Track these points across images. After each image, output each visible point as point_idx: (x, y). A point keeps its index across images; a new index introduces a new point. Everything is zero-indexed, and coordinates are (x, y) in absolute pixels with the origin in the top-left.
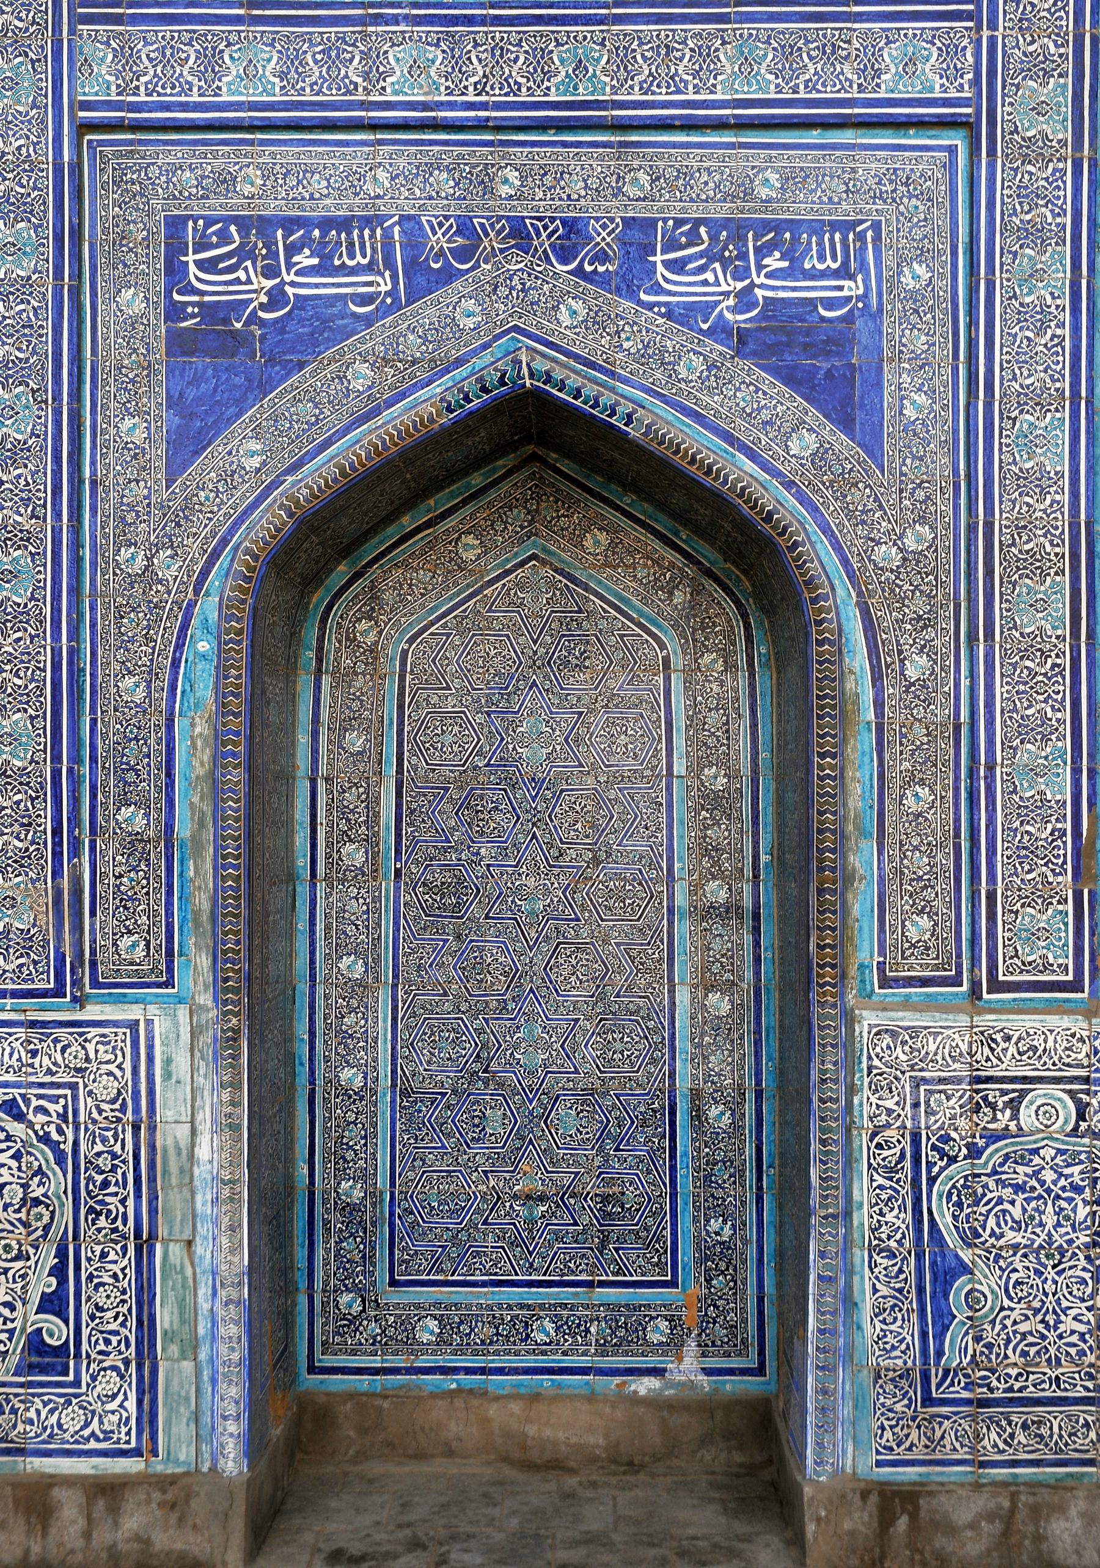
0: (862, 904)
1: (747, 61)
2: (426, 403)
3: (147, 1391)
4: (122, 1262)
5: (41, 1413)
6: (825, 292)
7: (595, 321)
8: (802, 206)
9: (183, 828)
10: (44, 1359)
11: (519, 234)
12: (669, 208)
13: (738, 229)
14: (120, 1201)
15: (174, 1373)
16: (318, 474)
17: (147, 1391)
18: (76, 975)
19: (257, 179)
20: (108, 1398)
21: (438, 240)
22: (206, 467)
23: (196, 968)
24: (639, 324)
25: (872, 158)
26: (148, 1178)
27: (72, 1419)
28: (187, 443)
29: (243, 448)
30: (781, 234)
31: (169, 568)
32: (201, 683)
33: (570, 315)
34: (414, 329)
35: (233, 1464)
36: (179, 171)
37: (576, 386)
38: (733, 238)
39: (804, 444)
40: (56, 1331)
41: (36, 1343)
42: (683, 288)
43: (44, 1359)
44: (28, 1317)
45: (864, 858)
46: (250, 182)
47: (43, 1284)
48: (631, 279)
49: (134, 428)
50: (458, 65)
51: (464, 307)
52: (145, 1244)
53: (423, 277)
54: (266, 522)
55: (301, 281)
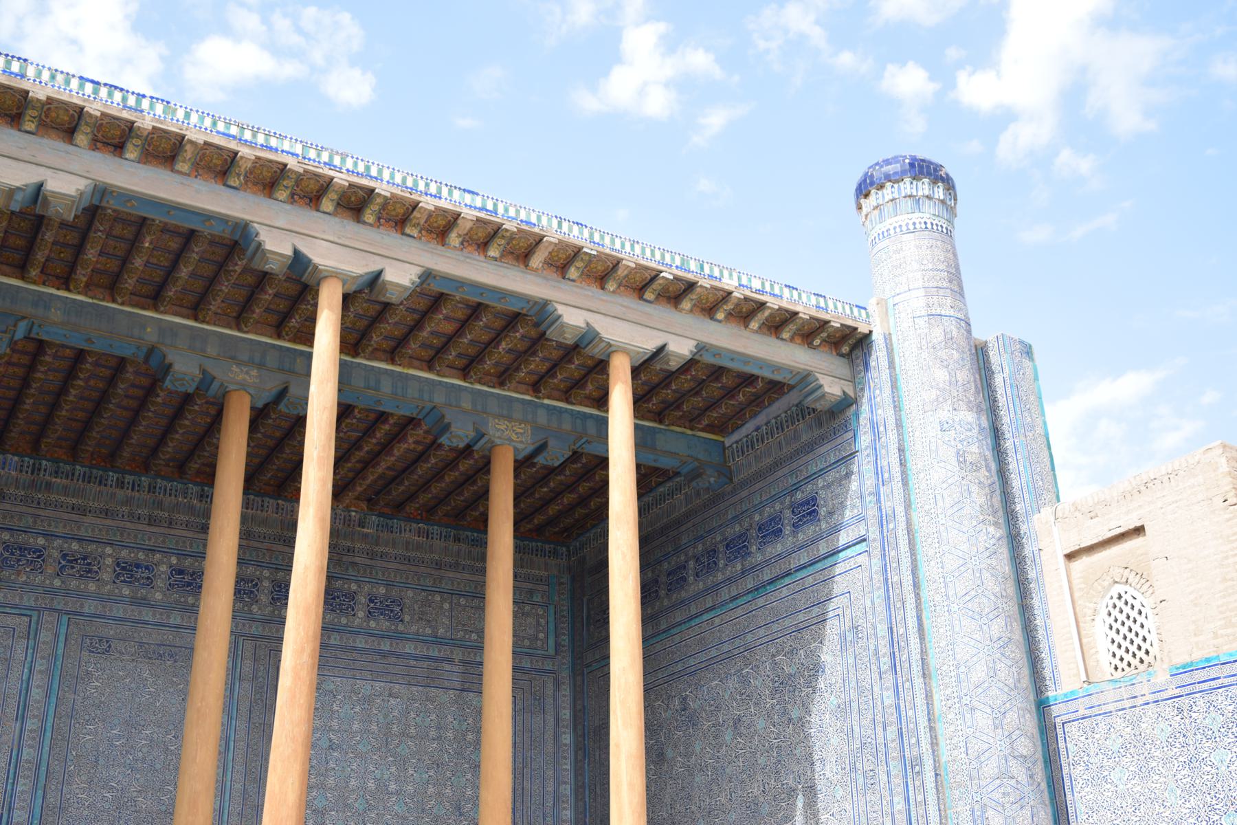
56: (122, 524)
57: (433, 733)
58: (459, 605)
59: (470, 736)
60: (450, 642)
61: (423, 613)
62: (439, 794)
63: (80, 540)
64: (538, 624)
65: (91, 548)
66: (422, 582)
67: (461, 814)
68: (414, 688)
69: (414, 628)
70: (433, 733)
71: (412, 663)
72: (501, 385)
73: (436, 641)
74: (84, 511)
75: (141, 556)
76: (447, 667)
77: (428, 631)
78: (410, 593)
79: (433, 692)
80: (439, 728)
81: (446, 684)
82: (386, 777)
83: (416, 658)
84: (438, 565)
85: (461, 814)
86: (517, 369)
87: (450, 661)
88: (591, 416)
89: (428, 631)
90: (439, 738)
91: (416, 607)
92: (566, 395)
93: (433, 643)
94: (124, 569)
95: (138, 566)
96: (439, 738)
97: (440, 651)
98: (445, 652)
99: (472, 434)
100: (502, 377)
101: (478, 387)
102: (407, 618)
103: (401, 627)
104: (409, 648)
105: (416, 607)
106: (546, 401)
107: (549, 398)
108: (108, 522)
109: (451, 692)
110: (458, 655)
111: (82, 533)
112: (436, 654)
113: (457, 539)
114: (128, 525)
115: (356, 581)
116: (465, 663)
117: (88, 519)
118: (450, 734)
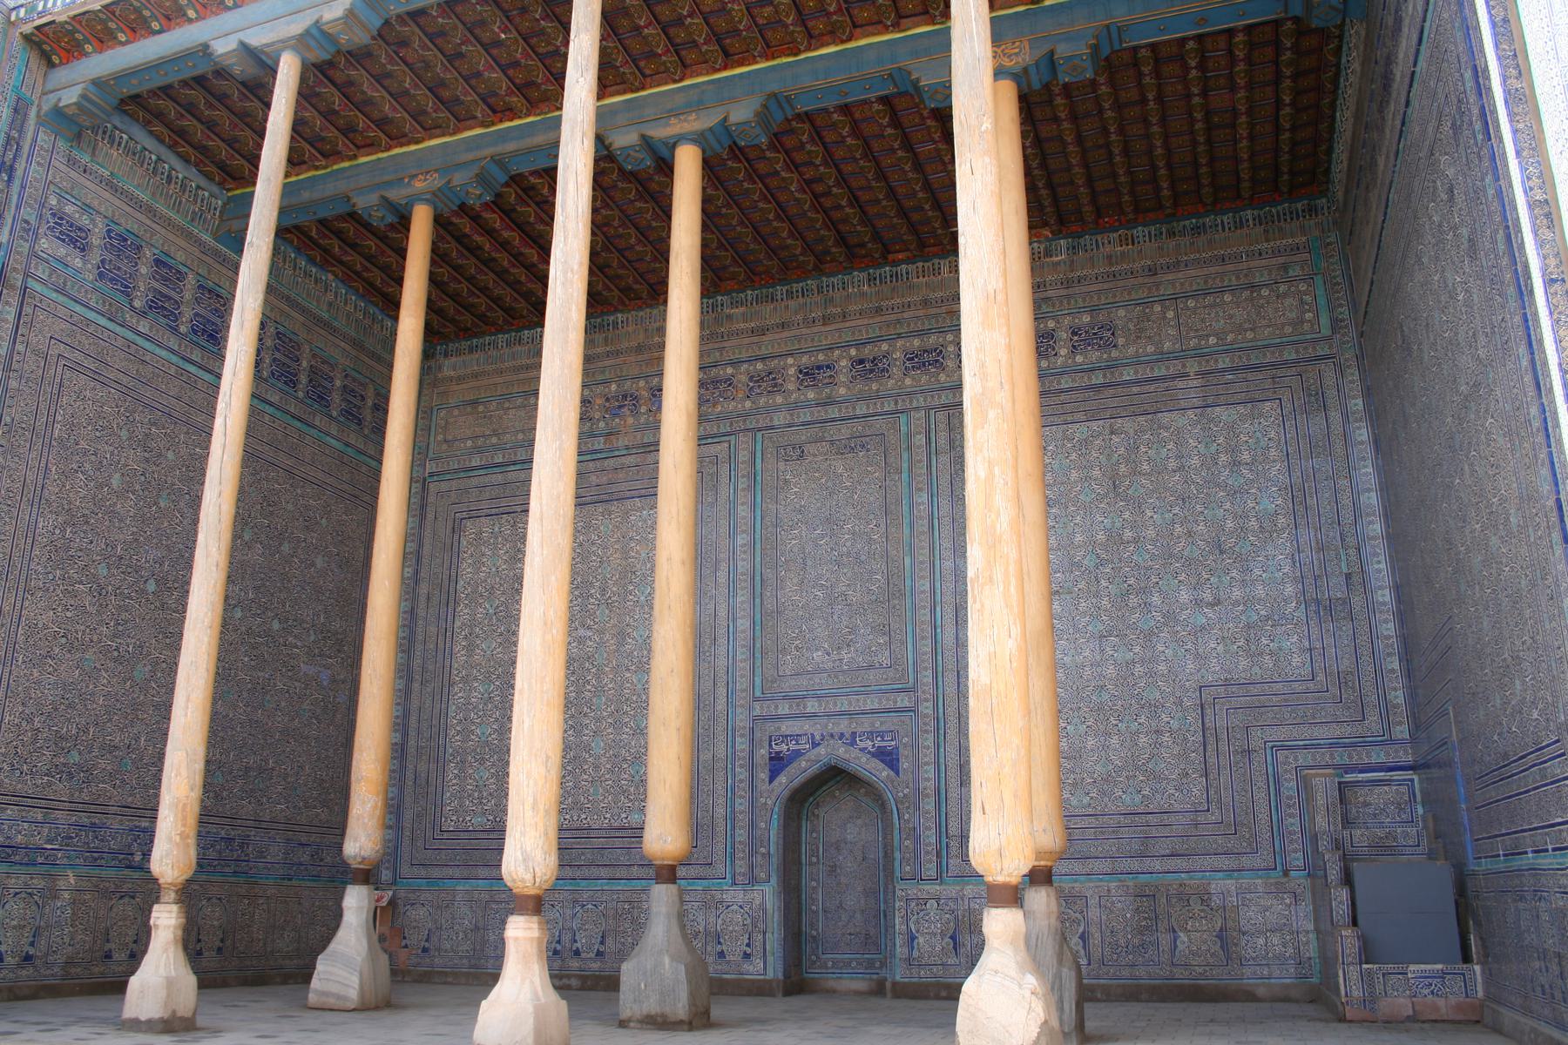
0: (897, 864)
2: (814, 770)
4: (760, 937)
5: (746, 967)
10: (747, 956)
11: (832, 736)
14: (761, 926)
15: (770, 959)
16: (796, 783)
18: (753, 880)
19: (786, 728)
21: (818, 738)
22: (776, 783)
23: (774, 880)
28: (771, 780)
29: (782, 779)
32: (775, 823)
34: (813, 754)
35: (781, 976)
36: (770, 727)
40: (749, 950)
45: (897, 855)
46: (784, 728)
49: (763, 775)
51: (822, 750)
53: (815, 745)
54: (786, 793)
55: (793, 746)
56: (797, 332)
57: (1172, 464)
58: (1188, 308)
60: (1182, 355)
61: (1141, 330)
62: (1190, 534)
64: (1302, 302)
65: (774, 363)
66: (1134, 296)
67: (1222, 552)
68: (1141, 418)
69: (1131, 350)
71: (1135, 390)
73: (1162, 357)
74: (763, 331)
75: (821, 357)
76: (1181, 385)
77: (1150, 349)
78: (1122, 313)
79: (1165, 418)
80: (1179, 457)
81: (1183, 404)
82: (1118, 525)
83: (1138, 382)
84: (1152, 271)
85: (1222, 552)
87: (1185, 375)
89: (1150, 349)
90: (1181, 468)
93: (1158, 361)
94: (806, 374)
95: (819, 368)
96: (1181, 468)
97: (1168, 368)
98: (1175, 367)
102: (1121, 341)
103: (1115, 353)
104: (1128, 375)
108: (786, 334)
109: (1190, 412)
110: (1193, 367)
111: (764, 351)
112: (1163, 372)
114: (804, 331)
115: (1053, 318)
116: (1202, 374)
118: (1195, 461)
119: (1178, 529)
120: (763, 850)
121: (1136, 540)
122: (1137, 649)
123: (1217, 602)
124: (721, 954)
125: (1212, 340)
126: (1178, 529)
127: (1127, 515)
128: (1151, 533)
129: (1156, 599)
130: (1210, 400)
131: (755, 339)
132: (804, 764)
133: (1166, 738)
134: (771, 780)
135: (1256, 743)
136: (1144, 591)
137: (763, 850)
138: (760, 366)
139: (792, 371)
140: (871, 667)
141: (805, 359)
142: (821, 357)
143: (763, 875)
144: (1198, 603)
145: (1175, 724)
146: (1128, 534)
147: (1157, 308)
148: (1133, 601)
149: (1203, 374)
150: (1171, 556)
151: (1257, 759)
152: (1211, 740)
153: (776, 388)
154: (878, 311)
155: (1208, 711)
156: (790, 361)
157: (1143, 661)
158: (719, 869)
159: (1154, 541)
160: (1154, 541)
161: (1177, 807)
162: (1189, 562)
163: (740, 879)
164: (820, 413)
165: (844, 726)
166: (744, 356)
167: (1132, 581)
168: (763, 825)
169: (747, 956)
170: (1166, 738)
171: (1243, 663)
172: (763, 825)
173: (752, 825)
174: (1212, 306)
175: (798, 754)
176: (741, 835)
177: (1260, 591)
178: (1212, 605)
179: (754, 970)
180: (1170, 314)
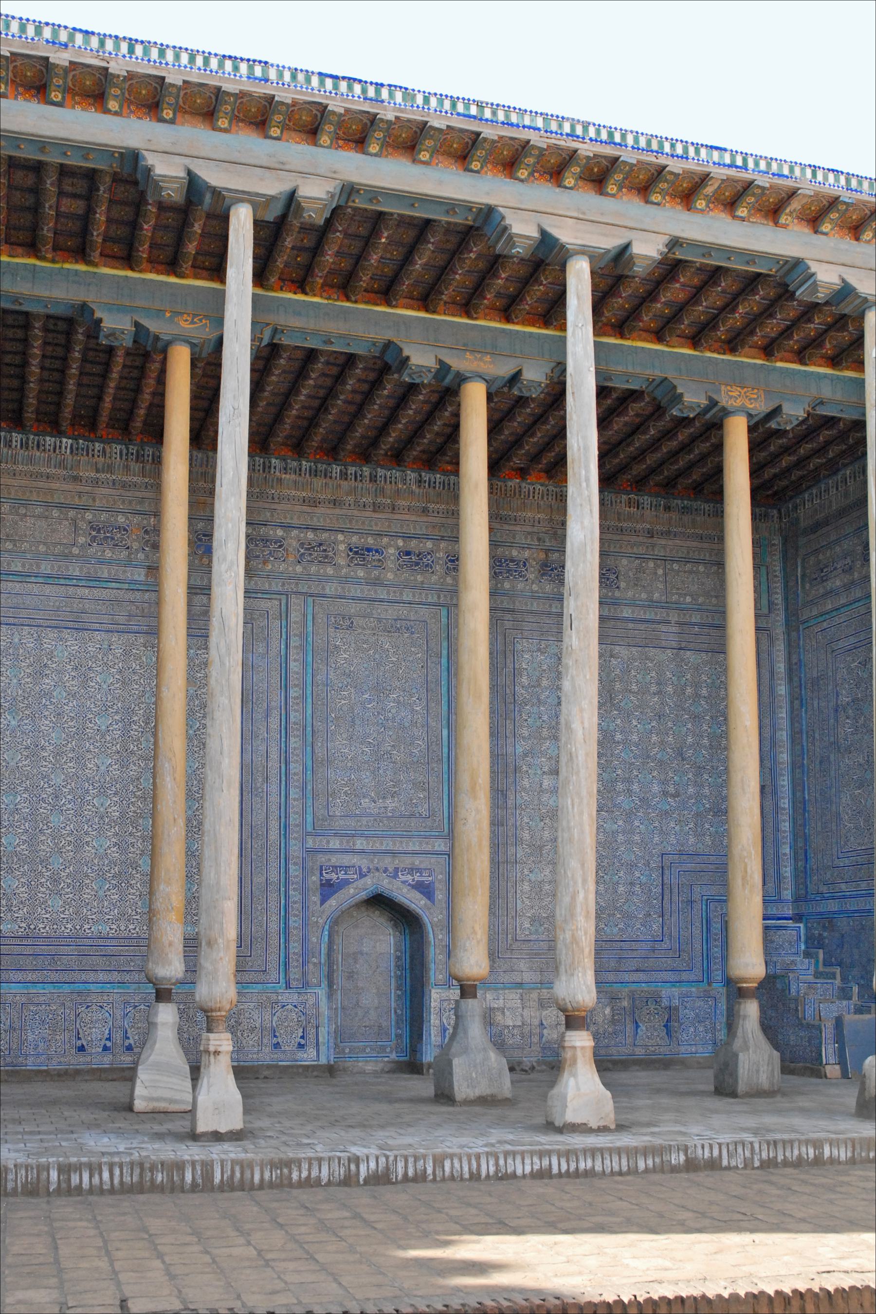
1: (414, 844)
3: (318, 1051)
5: (300, 1055)
6: (426, 879)
7: (389, 883)
8: (422, 866)
9: (323, 961)
11: (377, 869)
12: (402, 866)
13: (412, 869)
17: (318, 1051)
20: (312, 1053)
21: (365, 870)
24: (397, 883)
25: (433, 859)
26: (318, 1016)
27: (305, 1056)
29: (333, 902)
30: (419, 870)
31: (321, 921)
33: (386, 881)
34: (361, 883)
37: (387, 893)
38: (411, 870)
39: (422, 902)
40: (303, 1042)
41: (299, 1044)
42: (403, 878)
43: (301, 1046)
44: (298, 1040)
47: (301, 1034)
48: (395, 876)
50: (368, 844)
51: (368, 880)
52: (317, 1027)
56: (350, 513)
57: (654, 688)
58: (673, 570)
59: (689, 690)
61: (637, 579)
62: (662, 742)
63: (315, 529)
65: (325, 536)
66: (635, 550)
67: (683, 759)
68: (634, 649)
69: (630, 594)
70: (654, 688)
71: (631, 625)
72: (733, 350)
73: (652, 604)
74: (315, 503)
75: (370, 540)
77: (644, 596)
78: (625, 562)
79: (652, 652)
80: (659, 684)
81: (664, 644)
83: (634, 621)
84: (651, 534)
85: (683, 759)
86: (752, 333)
88: (825, 376)
89: (644, 596)
90: (659, 693)
91: (631, 574)
92: (801, 356)
93: (649, 607)
95: (369, 550)
96: (659, 693)
97: (656, 614)
98: (661, 614)
99: (704, 402)
100: (732, 345)
101: (709, 354)
102: (623, 585)
103: (617, 594)
104: (627, 613)
105: (631, 574)
106: (779, 364)
107: (781, 360)
108: (337, 511)
109: (668, 651)
110: (674, 617)
111: (315, 522)
112: (653, 617)
113: (667, 508)
114: (356, 513)
116: (680, 624)
117: (320, 510)
118: (670, 689)
119: (654, 738)
120: (315, 960)
121: (625, 742)
122: (620, 823)
123: (676, 795)
124: (277, 1045)
125: (688, 599)
126: (654, 738)
127: (619, 721)
128: (635, 738)
129: (635, 787)
130: (683, 645)
131: (309, 509)
132: (352, 891)
133: (637, 888)
134: (323, 902)
135: (696, 897)
136: (628, 781)
137: (315, 960)
138: (310, 535)
139: (342, 547)
140: (412, 816)
141: (355, 539)
142: (370, 540)
143: (315, 981)
144: (665, 794)
145: (644, 879)
146: (618, 737)
147: (651, 564)
148: (620, 786)
149: (680, 624)
150: (648, 757)
151: (697, 906)
152: (667, 892)
153: (326, 559)
154: (425, 511)
155: (667, 872)
156: (340, 537)
157: (624, 832)
158: (274, 976)
159: (637, 745)
160: (637, 745)
161: (642, 938)
162: (661, 763)
163: (294, 984)
164: (367, 591)
165: (388, 862)
166: (295, 522)
167: (619, 772)
168: (314, 940)
169: (301, 1046)
170: (637, 888)
171: (692, 840)
172: (314, 940)
173: (304, 940)
174: (691, 572)
175: (346, 883)
176: (295, 947)
177: (706, 791)
178: (674, 796)
179: (308, 1057)
180: (660, 572)
